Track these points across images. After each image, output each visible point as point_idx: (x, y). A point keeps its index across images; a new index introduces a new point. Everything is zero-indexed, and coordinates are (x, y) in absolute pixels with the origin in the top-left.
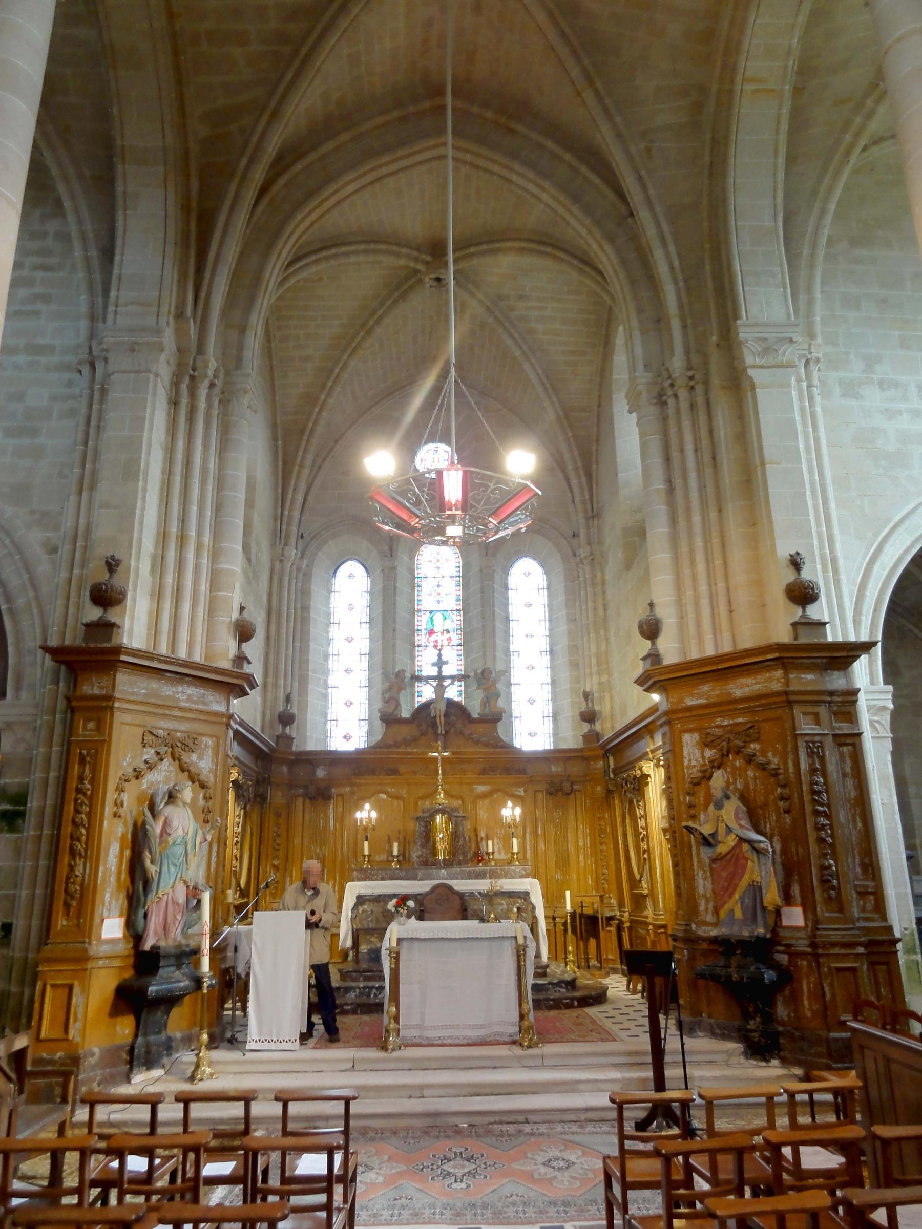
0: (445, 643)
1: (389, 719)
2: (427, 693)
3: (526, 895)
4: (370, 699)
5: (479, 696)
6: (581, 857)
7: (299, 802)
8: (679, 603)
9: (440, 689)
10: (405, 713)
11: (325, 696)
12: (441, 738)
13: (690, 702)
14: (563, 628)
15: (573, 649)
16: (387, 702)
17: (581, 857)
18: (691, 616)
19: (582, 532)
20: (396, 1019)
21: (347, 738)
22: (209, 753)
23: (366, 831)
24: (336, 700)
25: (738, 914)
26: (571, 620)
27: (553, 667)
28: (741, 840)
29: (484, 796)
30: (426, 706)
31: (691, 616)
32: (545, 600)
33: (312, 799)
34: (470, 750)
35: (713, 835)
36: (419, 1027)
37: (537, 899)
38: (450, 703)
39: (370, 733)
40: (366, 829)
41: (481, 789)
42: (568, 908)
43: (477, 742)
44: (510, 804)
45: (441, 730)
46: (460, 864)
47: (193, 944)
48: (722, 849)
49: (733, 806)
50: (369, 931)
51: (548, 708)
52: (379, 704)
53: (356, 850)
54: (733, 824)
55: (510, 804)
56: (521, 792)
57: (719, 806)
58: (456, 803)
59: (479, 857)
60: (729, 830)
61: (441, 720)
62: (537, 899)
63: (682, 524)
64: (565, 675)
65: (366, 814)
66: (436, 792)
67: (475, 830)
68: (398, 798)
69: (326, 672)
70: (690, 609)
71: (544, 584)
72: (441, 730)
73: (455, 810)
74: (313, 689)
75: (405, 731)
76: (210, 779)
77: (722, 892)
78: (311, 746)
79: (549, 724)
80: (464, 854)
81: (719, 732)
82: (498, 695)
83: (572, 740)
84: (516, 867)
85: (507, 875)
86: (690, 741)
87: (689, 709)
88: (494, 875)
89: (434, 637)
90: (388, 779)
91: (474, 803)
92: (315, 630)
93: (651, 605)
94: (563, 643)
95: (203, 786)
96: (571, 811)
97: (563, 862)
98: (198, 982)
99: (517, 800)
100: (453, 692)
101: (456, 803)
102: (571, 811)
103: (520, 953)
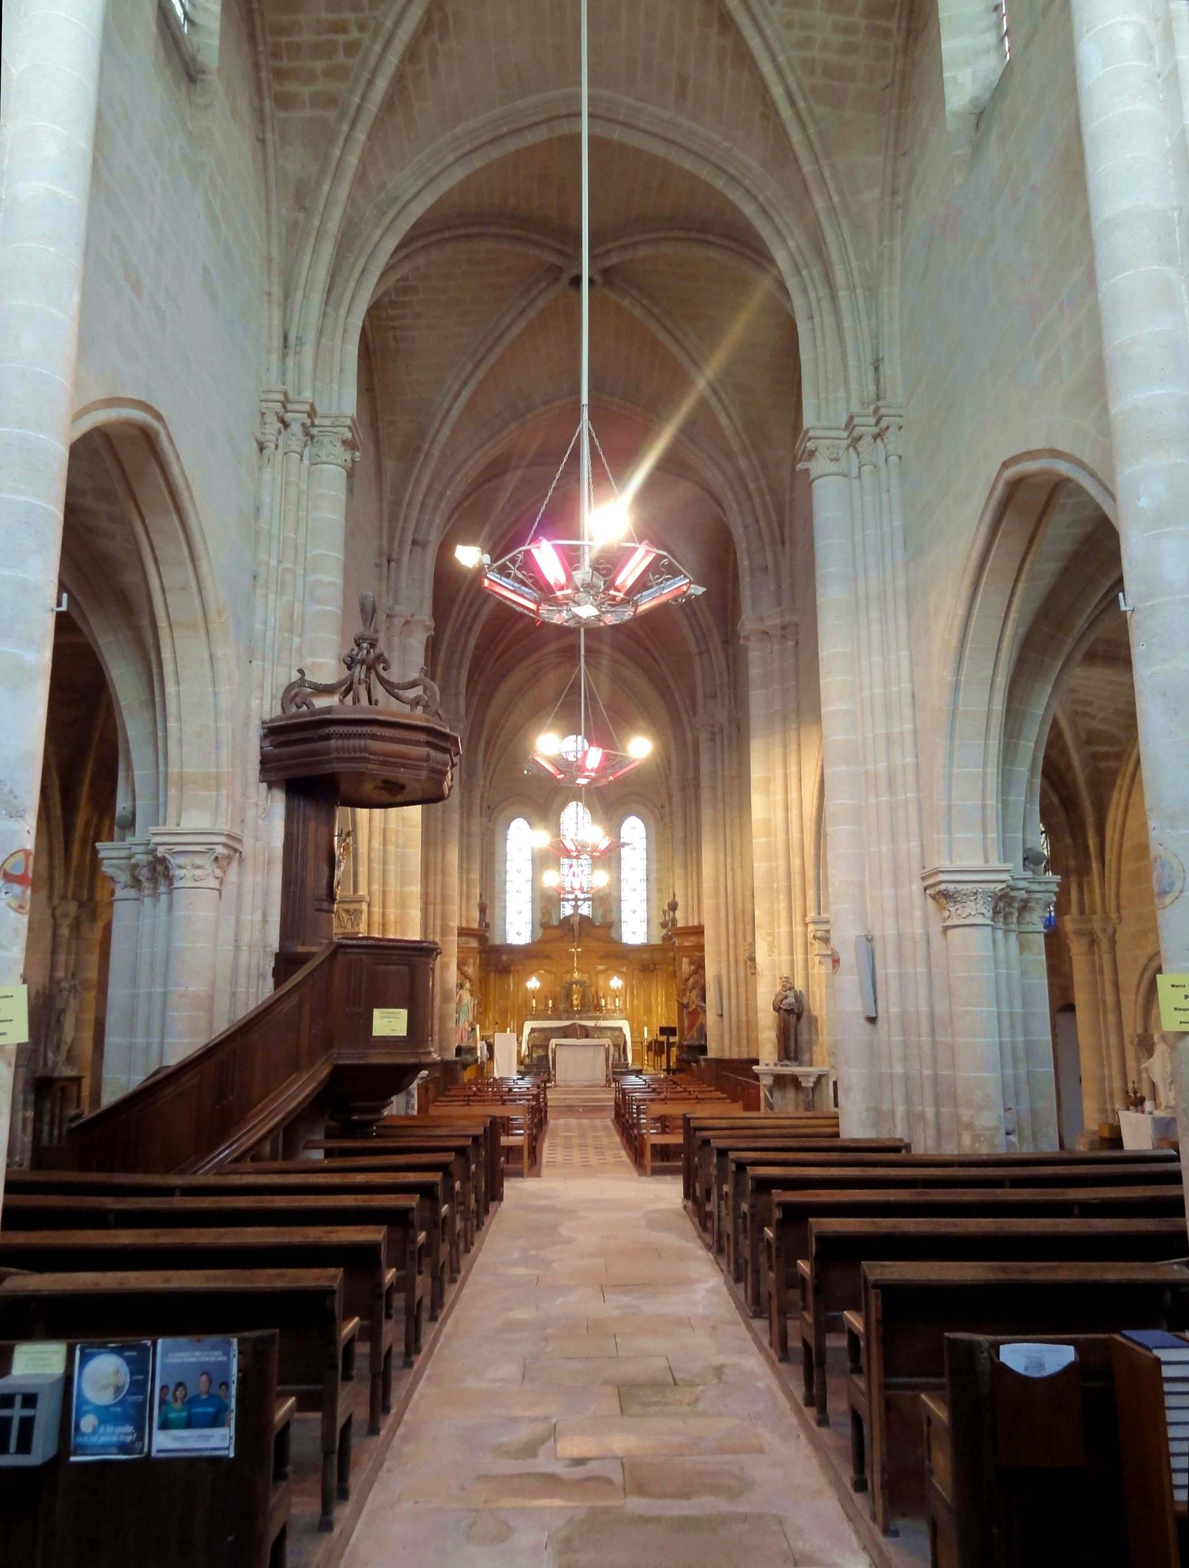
0: (580, 872)
1: (545, 926)
2: (567, 910)
3: (620, 1029)
4: (533, 909)
5: (600, 912)
6: (659, 1009)
7: (492, 975)
8: (686, 895)
9: (576, 907)
10: (555, 922)
11: (505, 908)
12: (576, 939)
13: (687, 944)
14: (654, 866)
15: (659, 880)
16: (543, 914)
17: (659, 1009)
18: (690, 902)
19: (667, 806)
20: (555, 1076)
21: (518, 934)
22: (471, 966)
23: (534, 994)
24: (511, 916)
25: (695, 1036)
26: (660, 861)
27: (648, 890)
28: (697, 1006)
29: (602, 972)
30: (567, 918)
31: (690, 902)
32: (644, 846)
33: (499, 973)
34: (595, 945)
35: (688, 1004)
36: (565, 1081)
37: (627, 1031)
38: (582, 916)
39: (533, 931)
40: (533, 992)
41: (600, 967)
42: (646, 1036)
43: (598, 940)
44: (615, 978)
45: (576, 933)
46: (586, 1012)
47: (472, 1045)
48: (690, 1009)
49: (695, 993)
50: (538, 1046)
51: (644, 916)
52: (539, 915)
53: (527, 1003)
54: (695, 999)
55: (615, 978)
56: (625, 969)
57: (690, 992)
58: (585, 977)
59: (598, 1007)
60: (693, 1002)
61: (576, 927)
62: (627, 1031)
63: (689, 857)
64: (654, 896)
65: (533, 984)
66: (571, 971)
67: (597, 992)
68: (550, 972)
69: (505, 893)
70: (690, 899)
71: (644, 834)
72: (576, 933)
73: (585, 982)
74: (498, 904)
75: (556, 933)
76: (472, 977)
77: (691, 1027)
78: (497, 941)
79: (644, 926)
80: (589, 1006)
81: (695, 958)
82: (611, 911)
83: (657, 941)
84: (617, 1014)
85: (611, 1018)
86: (685, 961)
87: (686, 947)
88: (605, 1019)
89: (573, 869)
90: (545, 961)
91: (597, 976)
92: (498, 866)
93: (674, 895)
94: (654, 876)
95: (470, 980)
96: (655, 982)
97: (648, 1011)
98: (477, 1060)
99: (621, 974)
100: (585, 910)
101: (585, 977)
102: (655, 982)
103: (607, 1050)
